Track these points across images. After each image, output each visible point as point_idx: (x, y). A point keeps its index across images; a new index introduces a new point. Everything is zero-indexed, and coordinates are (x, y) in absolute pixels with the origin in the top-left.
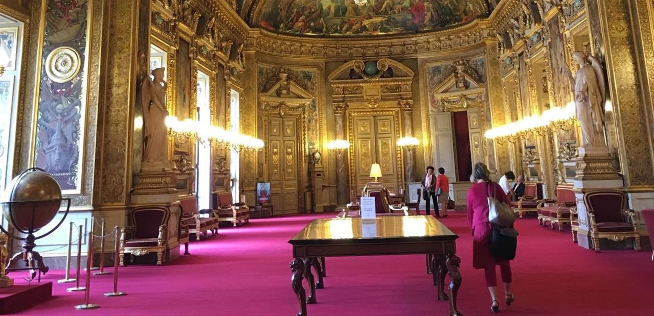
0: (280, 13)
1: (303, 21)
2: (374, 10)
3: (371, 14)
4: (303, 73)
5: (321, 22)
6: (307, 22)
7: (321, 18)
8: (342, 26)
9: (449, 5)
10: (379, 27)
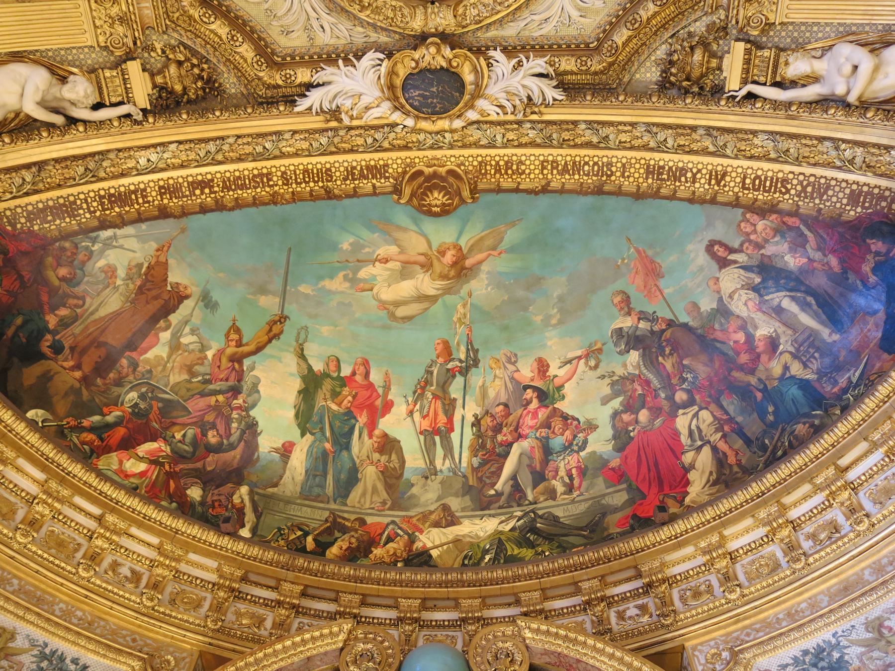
0: (42, 356)
1: (154, 461)
2: (467, 490)
3: (455, 504)
4: (43, 656)
5: (236, 499)
6: (170, 475)
7: (239, 484)
8: (324, 539)
9: (796, 369)
10: (487, 558)
